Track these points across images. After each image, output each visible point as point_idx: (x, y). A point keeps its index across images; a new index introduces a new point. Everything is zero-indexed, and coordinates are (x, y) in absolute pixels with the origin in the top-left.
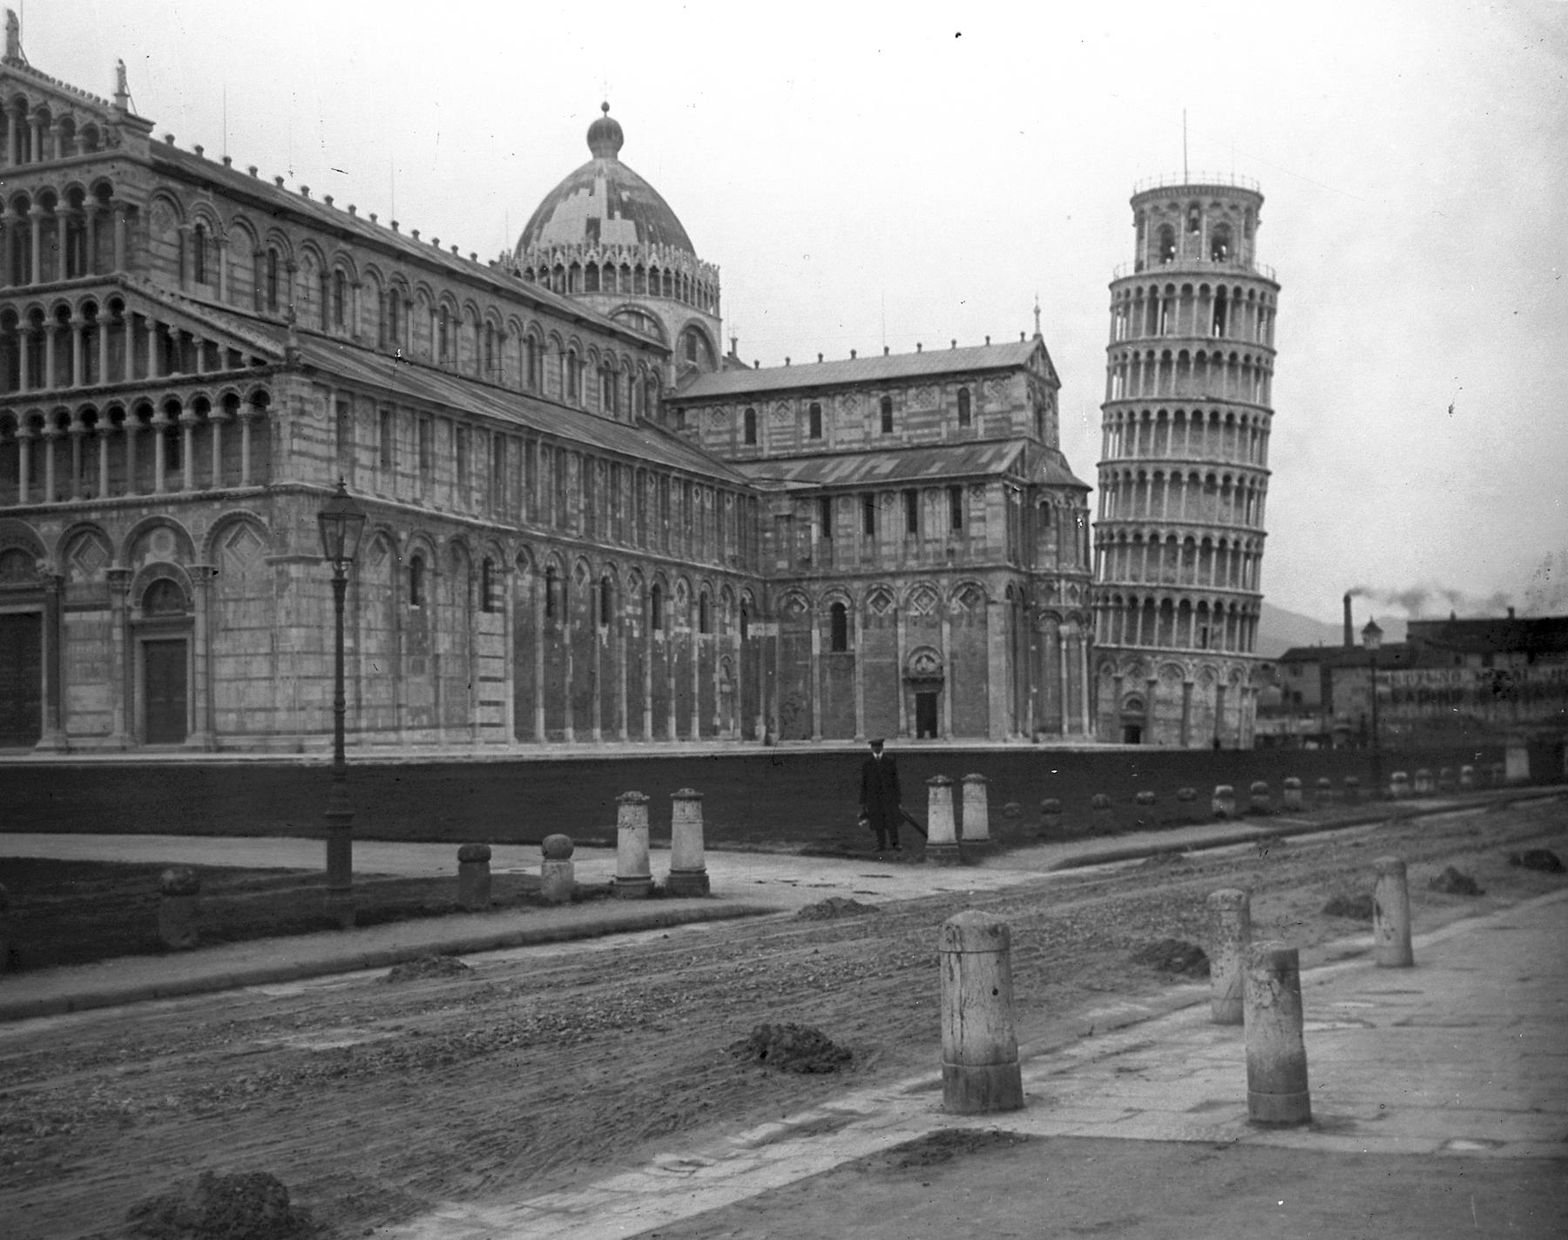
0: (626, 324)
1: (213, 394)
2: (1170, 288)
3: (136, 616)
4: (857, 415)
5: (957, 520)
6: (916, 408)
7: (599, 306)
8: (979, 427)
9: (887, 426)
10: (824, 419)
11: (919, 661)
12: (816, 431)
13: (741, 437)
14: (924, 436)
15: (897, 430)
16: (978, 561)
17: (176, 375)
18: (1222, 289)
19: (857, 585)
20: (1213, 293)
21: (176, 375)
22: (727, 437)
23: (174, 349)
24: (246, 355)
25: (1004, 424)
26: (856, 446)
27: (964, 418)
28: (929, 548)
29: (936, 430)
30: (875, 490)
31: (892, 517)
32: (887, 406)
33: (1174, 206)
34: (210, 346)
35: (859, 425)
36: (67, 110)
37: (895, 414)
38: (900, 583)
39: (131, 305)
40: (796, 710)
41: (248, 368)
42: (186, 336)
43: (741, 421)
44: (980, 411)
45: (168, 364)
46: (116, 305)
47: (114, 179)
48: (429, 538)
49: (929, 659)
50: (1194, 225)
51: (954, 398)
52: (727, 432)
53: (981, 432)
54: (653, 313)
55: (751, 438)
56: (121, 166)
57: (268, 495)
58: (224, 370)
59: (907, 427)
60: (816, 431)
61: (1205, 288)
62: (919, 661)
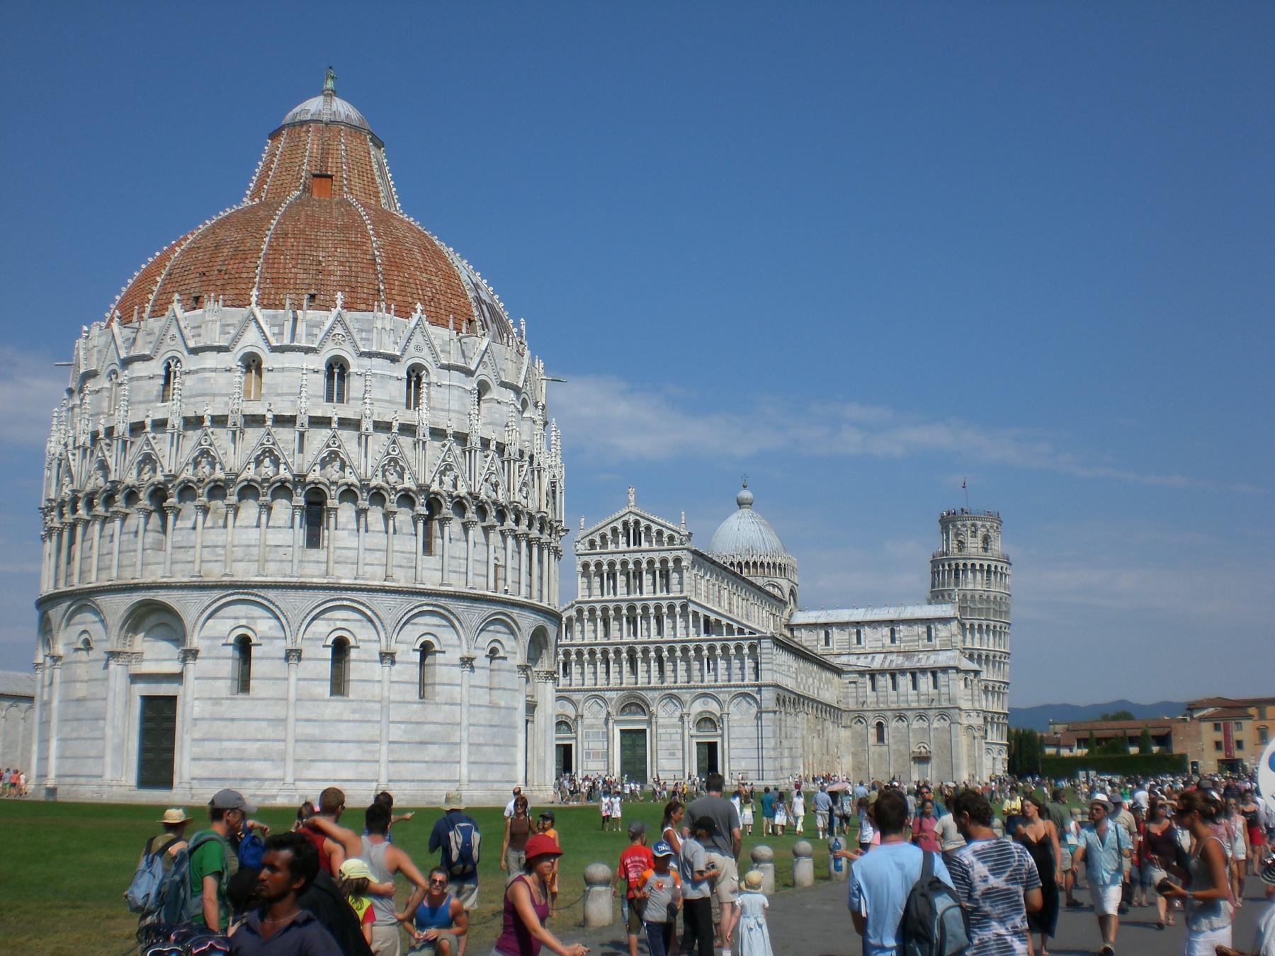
0: (770, 589)
1: (732, 645)
2: (965, 565)
4: (878, 636)
5: (935, 686)
7: (759, 581)
8: (936, 642)
9: (893, 640)
12: (859, 642)
16: (945, 704)
17: (714, 636)
18: (989, 566)
19: (889, 713)
21: (714, 636)
23: (709, 626)
24: (747, 631)
27: (930, 639)
31: (905, 682)
32: (893, 632)
33: (964, 526)
39: (691, 607)
42: (718, 621)
45: (707, 631)
46: (684, 607)
50: (974, 534)
55: (827, 643)
60: (859, 642)
61: (981, 565)
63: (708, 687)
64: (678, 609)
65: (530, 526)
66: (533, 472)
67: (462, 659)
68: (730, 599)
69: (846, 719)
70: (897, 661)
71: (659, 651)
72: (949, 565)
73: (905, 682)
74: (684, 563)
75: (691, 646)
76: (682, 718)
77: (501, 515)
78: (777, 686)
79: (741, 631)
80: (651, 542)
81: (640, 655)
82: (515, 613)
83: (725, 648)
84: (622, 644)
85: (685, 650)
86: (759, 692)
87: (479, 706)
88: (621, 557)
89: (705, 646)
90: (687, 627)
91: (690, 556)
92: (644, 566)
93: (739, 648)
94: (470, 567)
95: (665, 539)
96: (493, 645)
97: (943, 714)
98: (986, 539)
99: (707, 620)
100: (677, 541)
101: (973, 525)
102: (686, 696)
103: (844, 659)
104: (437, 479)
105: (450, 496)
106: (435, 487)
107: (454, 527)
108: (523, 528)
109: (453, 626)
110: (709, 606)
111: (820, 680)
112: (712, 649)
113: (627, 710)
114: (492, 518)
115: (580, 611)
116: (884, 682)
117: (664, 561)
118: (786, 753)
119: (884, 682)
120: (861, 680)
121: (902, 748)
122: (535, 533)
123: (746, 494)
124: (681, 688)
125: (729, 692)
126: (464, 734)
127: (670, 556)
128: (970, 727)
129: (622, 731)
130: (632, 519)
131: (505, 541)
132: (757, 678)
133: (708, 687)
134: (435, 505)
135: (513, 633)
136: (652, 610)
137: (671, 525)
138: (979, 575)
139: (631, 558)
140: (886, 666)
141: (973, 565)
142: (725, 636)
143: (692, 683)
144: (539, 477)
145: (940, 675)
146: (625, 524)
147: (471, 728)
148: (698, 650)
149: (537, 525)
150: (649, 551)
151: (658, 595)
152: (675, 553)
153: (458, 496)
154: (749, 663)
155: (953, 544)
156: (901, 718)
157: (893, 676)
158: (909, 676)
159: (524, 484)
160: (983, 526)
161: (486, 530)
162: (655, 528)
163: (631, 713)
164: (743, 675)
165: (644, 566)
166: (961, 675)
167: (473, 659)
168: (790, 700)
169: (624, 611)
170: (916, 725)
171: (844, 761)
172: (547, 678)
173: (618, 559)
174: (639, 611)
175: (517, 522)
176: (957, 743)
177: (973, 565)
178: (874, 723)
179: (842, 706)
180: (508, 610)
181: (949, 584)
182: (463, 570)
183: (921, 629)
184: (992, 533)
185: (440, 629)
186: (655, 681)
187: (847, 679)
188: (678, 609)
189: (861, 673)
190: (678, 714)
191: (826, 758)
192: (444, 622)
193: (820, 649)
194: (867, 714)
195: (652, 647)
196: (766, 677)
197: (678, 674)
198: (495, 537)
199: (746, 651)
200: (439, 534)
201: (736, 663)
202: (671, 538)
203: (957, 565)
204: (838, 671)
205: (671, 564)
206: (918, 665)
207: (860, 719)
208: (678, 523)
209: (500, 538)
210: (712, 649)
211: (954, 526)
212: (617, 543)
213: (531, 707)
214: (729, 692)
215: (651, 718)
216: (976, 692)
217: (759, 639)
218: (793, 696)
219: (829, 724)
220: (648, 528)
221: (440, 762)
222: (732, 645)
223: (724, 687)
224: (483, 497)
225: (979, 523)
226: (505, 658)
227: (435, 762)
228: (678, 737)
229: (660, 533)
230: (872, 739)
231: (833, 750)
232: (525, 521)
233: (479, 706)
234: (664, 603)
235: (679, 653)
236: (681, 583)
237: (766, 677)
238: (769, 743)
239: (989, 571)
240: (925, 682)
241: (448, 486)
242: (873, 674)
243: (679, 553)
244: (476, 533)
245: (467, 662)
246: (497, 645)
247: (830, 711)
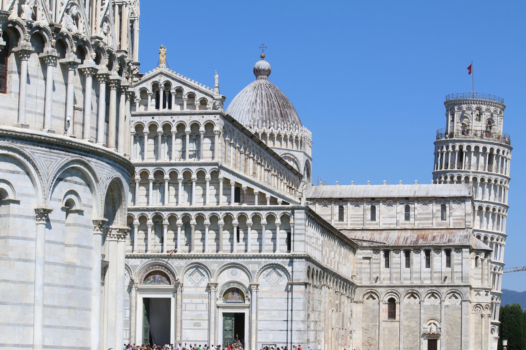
1: (264, 214)
2: (469, 147)
3: (220, 302)
5: (449, 263)
6: (421, 211)
9: (407, 218)
10: (377, 213)
11: (430, 324)
12: (373, 218)
13: (337, 217)
14: (425, 224)
15: (412, 220)
16: (458, 282)
17: (244, 205)
18: (492, 149)
19: (401, 290)
20: (488, 151)
21: (244, 205)
24: (280, 200)
25: (462, 221)
26: (392, 227)
28: (435, 275)
29: (431, 221)
30: (411, 249)
31: (418, 259)
32: (407, 209)
33: (469, 109)
34: (262, 196)
36: (193, 91)
37: (412, 213)
38: (421, 290)
39: (223, 174)
40: (370, 345)
41: (280, 205)
42: (250, 190)
45: (237, 200)
46: (215, 174)
47: (216, 122)
49: (434, 324)
52: (329, 215)
54: (295, 158)
55: (341, 218)
56: (218, 116)
57: (292, 259)
58: (268, 205)
60: (373, 218)
61: (485, 149)
62: (430, 324)
63: (237, 257)
64: (208, 176)
65: (110, 66)
66: (114, 6)
67: (37, 210)
68: (254, 169)
69: (359, 295)
70: (410, 238)
71: (186, 219)
72: (453, 147)
73: (418, 259)
74: (217, 128)
75: (221, 214)
76: (208, 288)
77: (81, 53)
78: (308, 258)
79: (274, 201)
80: (182, 105)
81: (166, 222)
82: (93, 162)
83: (256, 218)
84: (148, 210)
85: (214, 219)
86: (291, 264)
87: (55, 264)
88: (149, 119)
89: (235, 214)
90: (217, 195)
91: (222, 122)
92: (174, 129)
93: (271, 218)
94: (48, 108)
95: (197, 103)
96: (69, 197)
97: (455, 292)
98: (490, 122)
99: (238, 188)
100: (210, 105)
101: (479, 109)
102: (214, 265)
103: (359, 235)
104: (16, 6)
105: (30, 26)
106: (13, 16)
107: (32, 63)
108: (102, 68)
109: (28, 173)
110: (236, 171)
111: (340, 255)
112: (242, 218)
113: (151, 278)
114: (71, 56)
116: (398, 259)
117: (195, 126)
118: (312, 325)
119: (398, 259)
120: (374, 256)
122: (114, 75)
123: (263, 64)
124: (209, 257)
125: (259, 263)
126: (39, 294)
127: (202, 120)
128: (478, 305)
129: (147, 301)
130: (162, 80)
131: (83, 83)
132: (289, 249)
133: (237, 257)
134: (12, 36)
135: (89, 184)
136: (180, 176)
137: (203, 88)
138: (482, 158)
139: (160, 121)
140: (401, 243)
141: (477, 148)
142: (256, 205)
143: (220, 253)
144: (120, 14)
145: (453, 253)
146: (155, 85)
147: (46, 288)
148: (228, 218)
149: (116, 66)
150: (179, 114)
151: (188, 160)
152: (207, 118)
153: (38, 27)
154: (282, 234)
155: (458, 127)
156: (413, 295)
157: (408, 254)
158: (423, 254)
159: (106, 19)
160: (488, 110)
161: (65, 68)
162: (186, 90)
163: (154, 281)
164: (275, 245)
165: (174, 129)
166: (473, 255)
167: (50, 211)
168: (319, 272)
169: (151, 176)
170: (429, 302)
171: (354, 335)
172: (119, 237)
173: (147, 121)
174: (167, 176)
175: (97, 60)
176: (467, 320)
177: (477, 148)
178: (386, 299)
179: (357, 282)
180: (85, 159)
181: (453, 166)
182: (40, 110)
183: (436, 208)
184: (496, 118)
185: (15, 176)
186: (182, 249)
187: (361, 254)
188: (208, 176)
189: (376, 250)
190: (204, 284)
191: (342, 332)
192: (18, 169)
193: (335, 223)
194: (380, 290)
195: (179, 214)
196: (298, 249)
197: (205, 243)
198: (74, 77)
199: (278, 221)
200: (15, 69)
201: (267, 234)
202: (203, 102)
203: (461, 147)
204: (351, 245)
205: (202, 129)
206: (433, 243)
207: (372, 294)
208: (212, 86)
209: (78, 76)
210: (242, 218)
211: (460, 109)
212: (146, 105)
213: (105, 268)
214: (259, 263)
215: (176, 286)
216: (486, 272)
217: (293, 209)
218: (319, 270)
219: (344, 299)
220: (179, 91)
221: (13, 325)
222: (264, 214)
223: (254, 257)
224: (64, 30)
225: (484, 107)
226: (80, 212)
227: (8, 324)
228: (204, 307)
229: (191, 96)
230: (384, 315)
231: (348, 325)
232: (105, 61)
233: (55, 264)
234: (194, 170)
235: (207, 222)
236: (212, 149)
237: (298, 249)
238: (299, 316)
239: (491, 155)
240: (439, 260)
241: (27, 16)
242: (387, 251)
243: (211, 118)
244: (54, 72)
245: (43, 214)
246: (73, 197)
247: (347, 284)
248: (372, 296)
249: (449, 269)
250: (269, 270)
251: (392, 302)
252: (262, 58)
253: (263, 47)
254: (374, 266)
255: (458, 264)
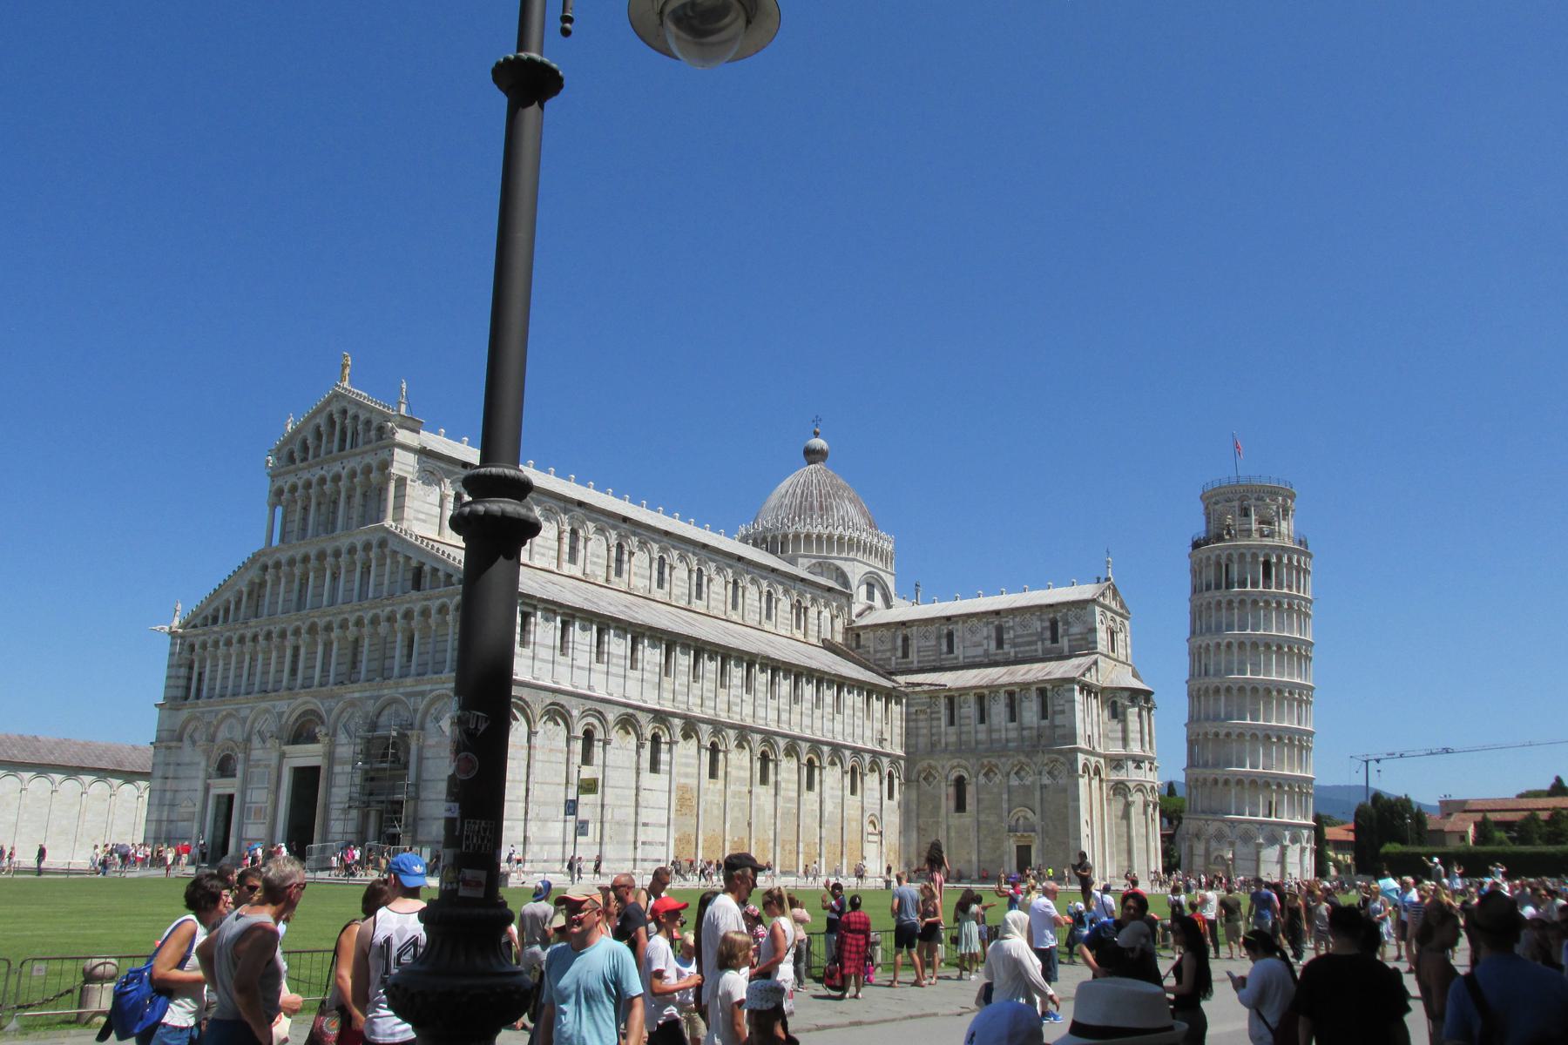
5: (1044, 716)
6: (1020, 631)
8: (1064, 643)
9: (1000, 643)
12: (951, 650)
13: (899, 653)
22: (888, 654)
27: (1054, 639)
28: (1025, 733)
31: (998, 710)
32: (1000, 630)
35: (981, 645)
43: (899, 642)
44: (1066, 633)
48: (601, 717)
51: (1047, 624)
53: (1066, 649)
55: (905, 655)
59: (1015, 645)
115: (265, 568)
121: (993, 819)
123: (819, 443)
125: (422, 694)
170: (1014, 782)
178: (954, 775)
242: (952, 699)
248: (930, 774)
249: (1045, 723)
250: (438, 705)
251: (960, 783)
252: (816, 434)
253: (817, 420)
254: (935, 723)
255: (1063, 712)
